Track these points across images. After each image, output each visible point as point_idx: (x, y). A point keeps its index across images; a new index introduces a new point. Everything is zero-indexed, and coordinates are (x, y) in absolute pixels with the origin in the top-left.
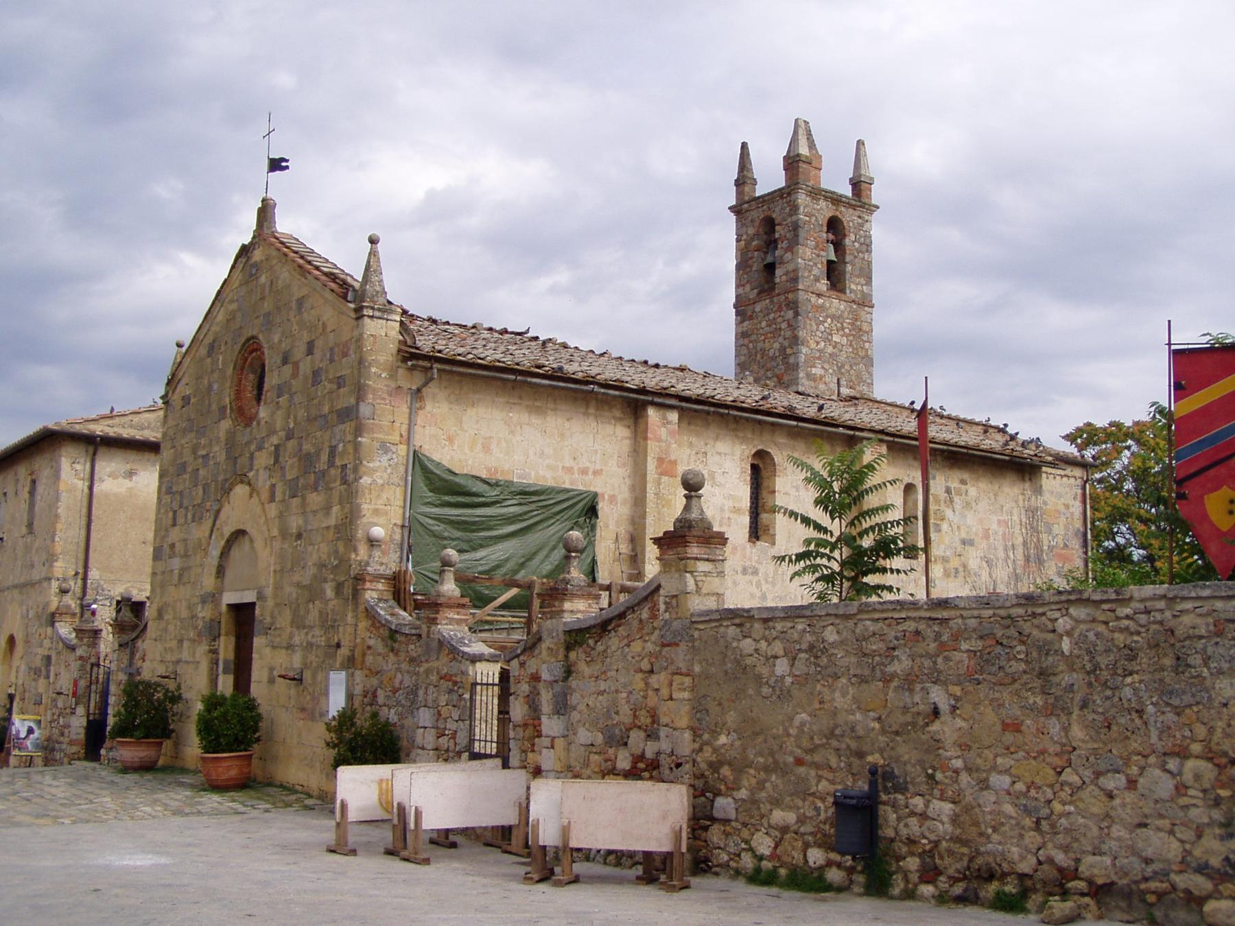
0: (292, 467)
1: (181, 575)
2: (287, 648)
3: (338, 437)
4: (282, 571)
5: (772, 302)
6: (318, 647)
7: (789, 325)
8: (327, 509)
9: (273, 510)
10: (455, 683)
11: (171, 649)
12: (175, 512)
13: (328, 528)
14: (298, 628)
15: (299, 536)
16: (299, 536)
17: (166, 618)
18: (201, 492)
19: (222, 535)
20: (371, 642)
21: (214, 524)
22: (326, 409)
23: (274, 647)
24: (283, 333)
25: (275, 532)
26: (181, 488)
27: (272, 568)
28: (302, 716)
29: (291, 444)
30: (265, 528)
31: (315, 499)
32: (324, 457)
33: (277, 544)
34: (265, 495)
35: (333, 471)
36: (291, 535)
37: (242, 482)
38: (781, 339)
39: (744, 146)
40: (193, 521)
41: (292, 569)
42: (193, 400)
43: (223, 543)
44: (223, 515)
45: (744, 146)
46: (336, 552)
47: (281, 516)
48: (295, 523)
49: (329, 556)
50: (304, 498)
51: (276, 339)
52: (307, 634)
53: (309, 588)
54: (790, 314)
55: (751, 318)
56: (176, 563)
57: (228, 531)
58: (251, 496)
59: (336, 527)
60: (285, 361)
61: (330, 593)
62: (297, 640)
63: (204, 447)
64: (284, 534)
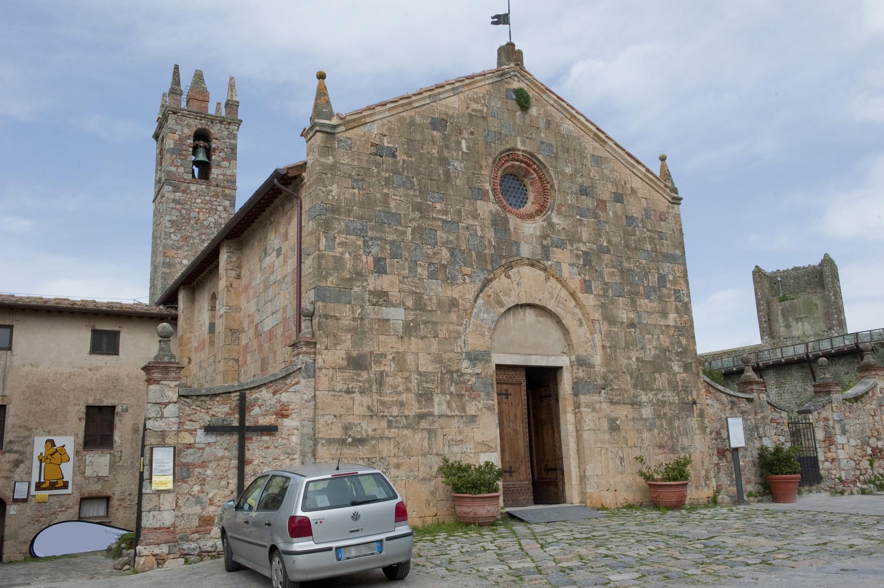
0: (613, 274)
1: (410, 329)
2: (633, 404)
3: (666, 270)
4: (614, 347)
5: (208, 188)
6: (670, 404)
7: (225, 209)
8: (664, 314)
9: (589, 300)
10: (778, 424)
11: (402, 404)
12: (378, 261)
13: (667, 326)
14: (644, 390)
15: (632, 325)
16: (632, 325)
17: (374, 368)
18: (445, 253)
19: (500, 303)
20: (709, 402)
21: (481, 291)
22: (649, 247)
23: (612, 402)
24: (576, 171)
25: (597, 316)
26: (391, 237)
27: (599, 344)
28: (661, 451)
29: (606, 257)
30: (577, 311)
31: (643, 302)
32: (653, 280)
33: (605, 327)
34: (575, 283)
35: (665, 291)
36: (622, 323)
37: (533, 265)
38: (216, 217)
39: (177, 67)
40: (432, 275)
41: (627, 347)
42: (401, 157)
43: (503, 310)
44: (495, 283)
45: (177, 67)
46: (680, 344)
47: (603, 306)
48: (624, 315)
49: (672, 343)
50: (633, 302)
51: (568, 170)
52: (656, 395)
53: (652, 363)
54: (227, 203)
55: (184, 192)
56: (397, 315)
57: (509, 302)
58: (547, 279)
59: (675, 327)
60: (584, 191)
61: (676, 368)
62: (644, 397)
63: (446, 213)
64: (610, 320)
